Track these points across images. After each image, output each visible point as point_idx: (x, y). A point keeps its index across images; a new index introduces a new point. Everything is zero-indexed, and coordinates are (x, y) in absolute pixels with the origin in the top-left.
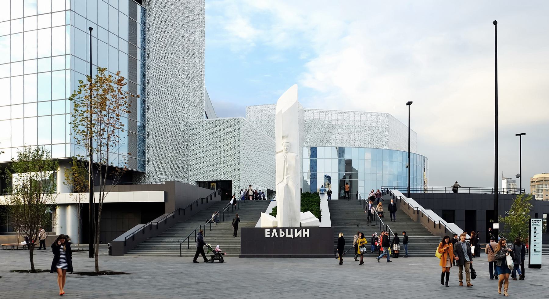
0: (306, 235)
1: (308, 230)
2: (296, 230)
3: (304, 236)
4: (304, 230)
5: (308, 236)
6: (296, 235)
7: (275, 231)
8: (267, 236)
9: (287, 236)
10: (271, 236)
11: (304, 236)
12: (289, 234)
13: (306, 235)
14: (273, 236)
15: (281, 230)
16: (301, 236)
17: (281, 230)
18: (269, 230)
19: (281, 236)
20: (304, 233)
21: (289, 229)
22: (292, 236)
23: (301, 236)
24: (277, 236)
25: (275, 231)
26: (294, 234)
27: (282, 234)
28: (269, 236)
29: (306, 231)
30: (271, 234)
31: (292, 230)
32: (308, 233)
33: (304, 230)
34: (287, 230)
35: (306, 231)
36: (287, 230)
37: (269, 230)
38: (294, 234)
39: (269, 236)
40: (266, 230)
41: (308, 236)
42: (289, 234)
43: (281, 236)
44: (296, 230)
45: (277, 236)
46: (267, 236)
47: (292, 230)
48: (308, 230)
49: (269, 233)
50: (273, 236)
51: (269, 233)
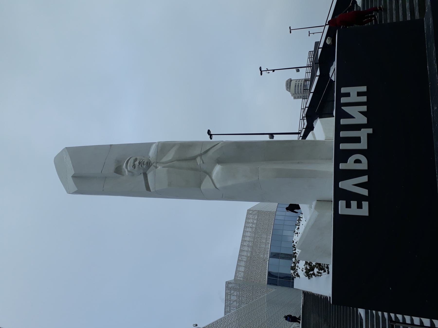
0: (359, 94)
1: (344, 90)
2: (343, 122)
3: (364, 99)
4: (343, 100)
5: (364, 89)
6: (363, 120)
7: (347, 185)
8: (365, 211)
9: (363, 145)
11: (364, 99)
12: (357, 140)
13: (359, 94)
14: (364, 192)
15: (342, 166)
16: (364, 108)
17: (342, 166)
19: (364, 166)
20: (354, 98)
21: (338, 140)
22: (363, 134)
23: (364, 108)
24: (364, 179)
25: (347, 185)
26: (358, 127)
27: (357, 161)
28: (365, 204)
29: (348, 95)
30: (360, 199)
31: (343, 134)
32: (353, 91)
33: (343, 100)
34: (343, 146)
35: (348, 95)
36: (343, 146)
37: (342, 203)
38: (358, 127)
39: (365, 204)
40: (343, 210)
41: (364, 89)
42: (357, 140)
43: (364, 166)
44: (343, 122)
45: (364, 179)
46: (365, 211)
47: (343, 134)
48: (344, 90)
49: (354, 204)
50: (364, 192)
51: (354, 204)
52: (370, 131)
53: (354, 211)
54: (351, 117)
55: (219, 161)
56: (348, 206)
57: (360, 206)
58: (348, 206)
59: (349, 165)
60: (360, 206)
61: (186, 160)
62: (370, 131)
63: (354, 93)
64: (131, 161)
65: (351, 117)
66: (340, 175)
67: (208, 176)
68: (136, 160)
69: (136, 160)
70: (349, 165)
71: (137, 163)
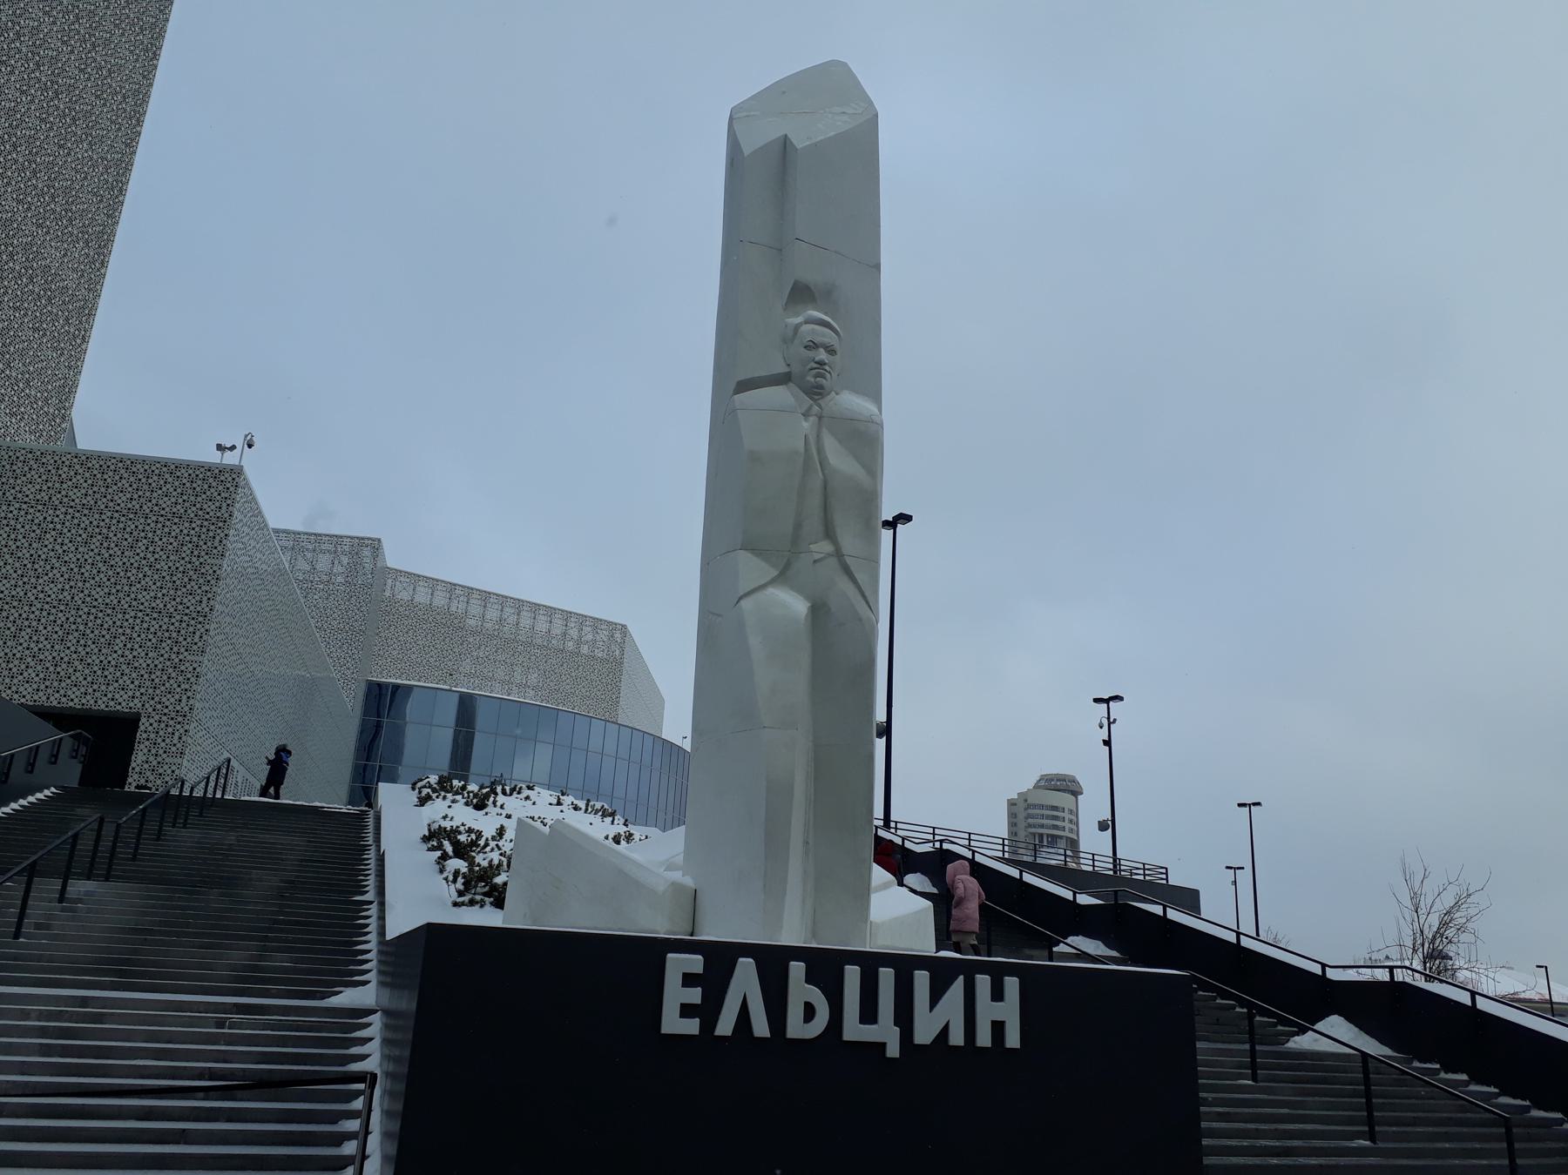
0: (998, 1028)
1: (1012, 984)
2: (922, 979)
3: (984, 1039)
4: (983, 982)
5: (1013, 1040)
6: (924, 1034)
7: (745, 980)
8: (673, 1023)
9: (853, 1030)
10: (709, 1021)
11: (984, 1039)
12: (869, 1014)
13: (998, 1028)
15: (797, 969)
16: (957, 1038)
17: (797, 969)
18: (695, 963)
19: (796, 1028)
20: (987, 1011)
21: (870, 963)
22: (885, 1032)
23: (957, 1038)
24: (761, 1028)
25: (745, 980)
26: (904, 1017)
27: (809, 1012)
28: (692, 1027)
29: (998, 994)
30: (707, 1011)
31: (886, 976)
32: (1009, 1011)
33: (983, 982)
34: (852, 974)
35: (998, 994)
36: (852, 974)
37: (695, 963)
38: (904, 1017)
39: (692, 1027)
40: (678, 964)
41: (1013, 1040)
42: (869, 1014)
43: (796, 1028)
44: (922, 979)
45: (761, 1028)
46: (673, 1023)
47: (886, 976)
48: (1012, 984)
49: (694, 995)
51: (694, 995)
52: (893, 1051)
53: (676, 994)
54: (935, 997)
55: (818, 610)
56: (689, 980)
57: (687, 1011)
58: (689, 980)
59: (800, 989)
60: (687, 1011)
61: (826, 507)
62: (893, 1051)
63: (1003, 1012)
64: (825, 335)
65: (935, 997)
66: (773, 962)
67: (776, 573)
68: (831, 351)
69: (831, 351)
70: (800, 989)
71: (822, 355)
